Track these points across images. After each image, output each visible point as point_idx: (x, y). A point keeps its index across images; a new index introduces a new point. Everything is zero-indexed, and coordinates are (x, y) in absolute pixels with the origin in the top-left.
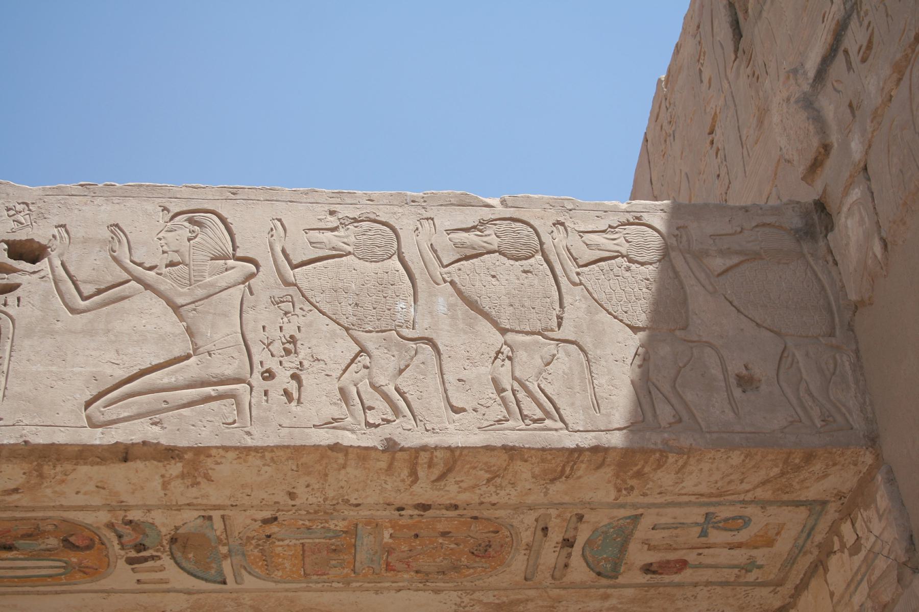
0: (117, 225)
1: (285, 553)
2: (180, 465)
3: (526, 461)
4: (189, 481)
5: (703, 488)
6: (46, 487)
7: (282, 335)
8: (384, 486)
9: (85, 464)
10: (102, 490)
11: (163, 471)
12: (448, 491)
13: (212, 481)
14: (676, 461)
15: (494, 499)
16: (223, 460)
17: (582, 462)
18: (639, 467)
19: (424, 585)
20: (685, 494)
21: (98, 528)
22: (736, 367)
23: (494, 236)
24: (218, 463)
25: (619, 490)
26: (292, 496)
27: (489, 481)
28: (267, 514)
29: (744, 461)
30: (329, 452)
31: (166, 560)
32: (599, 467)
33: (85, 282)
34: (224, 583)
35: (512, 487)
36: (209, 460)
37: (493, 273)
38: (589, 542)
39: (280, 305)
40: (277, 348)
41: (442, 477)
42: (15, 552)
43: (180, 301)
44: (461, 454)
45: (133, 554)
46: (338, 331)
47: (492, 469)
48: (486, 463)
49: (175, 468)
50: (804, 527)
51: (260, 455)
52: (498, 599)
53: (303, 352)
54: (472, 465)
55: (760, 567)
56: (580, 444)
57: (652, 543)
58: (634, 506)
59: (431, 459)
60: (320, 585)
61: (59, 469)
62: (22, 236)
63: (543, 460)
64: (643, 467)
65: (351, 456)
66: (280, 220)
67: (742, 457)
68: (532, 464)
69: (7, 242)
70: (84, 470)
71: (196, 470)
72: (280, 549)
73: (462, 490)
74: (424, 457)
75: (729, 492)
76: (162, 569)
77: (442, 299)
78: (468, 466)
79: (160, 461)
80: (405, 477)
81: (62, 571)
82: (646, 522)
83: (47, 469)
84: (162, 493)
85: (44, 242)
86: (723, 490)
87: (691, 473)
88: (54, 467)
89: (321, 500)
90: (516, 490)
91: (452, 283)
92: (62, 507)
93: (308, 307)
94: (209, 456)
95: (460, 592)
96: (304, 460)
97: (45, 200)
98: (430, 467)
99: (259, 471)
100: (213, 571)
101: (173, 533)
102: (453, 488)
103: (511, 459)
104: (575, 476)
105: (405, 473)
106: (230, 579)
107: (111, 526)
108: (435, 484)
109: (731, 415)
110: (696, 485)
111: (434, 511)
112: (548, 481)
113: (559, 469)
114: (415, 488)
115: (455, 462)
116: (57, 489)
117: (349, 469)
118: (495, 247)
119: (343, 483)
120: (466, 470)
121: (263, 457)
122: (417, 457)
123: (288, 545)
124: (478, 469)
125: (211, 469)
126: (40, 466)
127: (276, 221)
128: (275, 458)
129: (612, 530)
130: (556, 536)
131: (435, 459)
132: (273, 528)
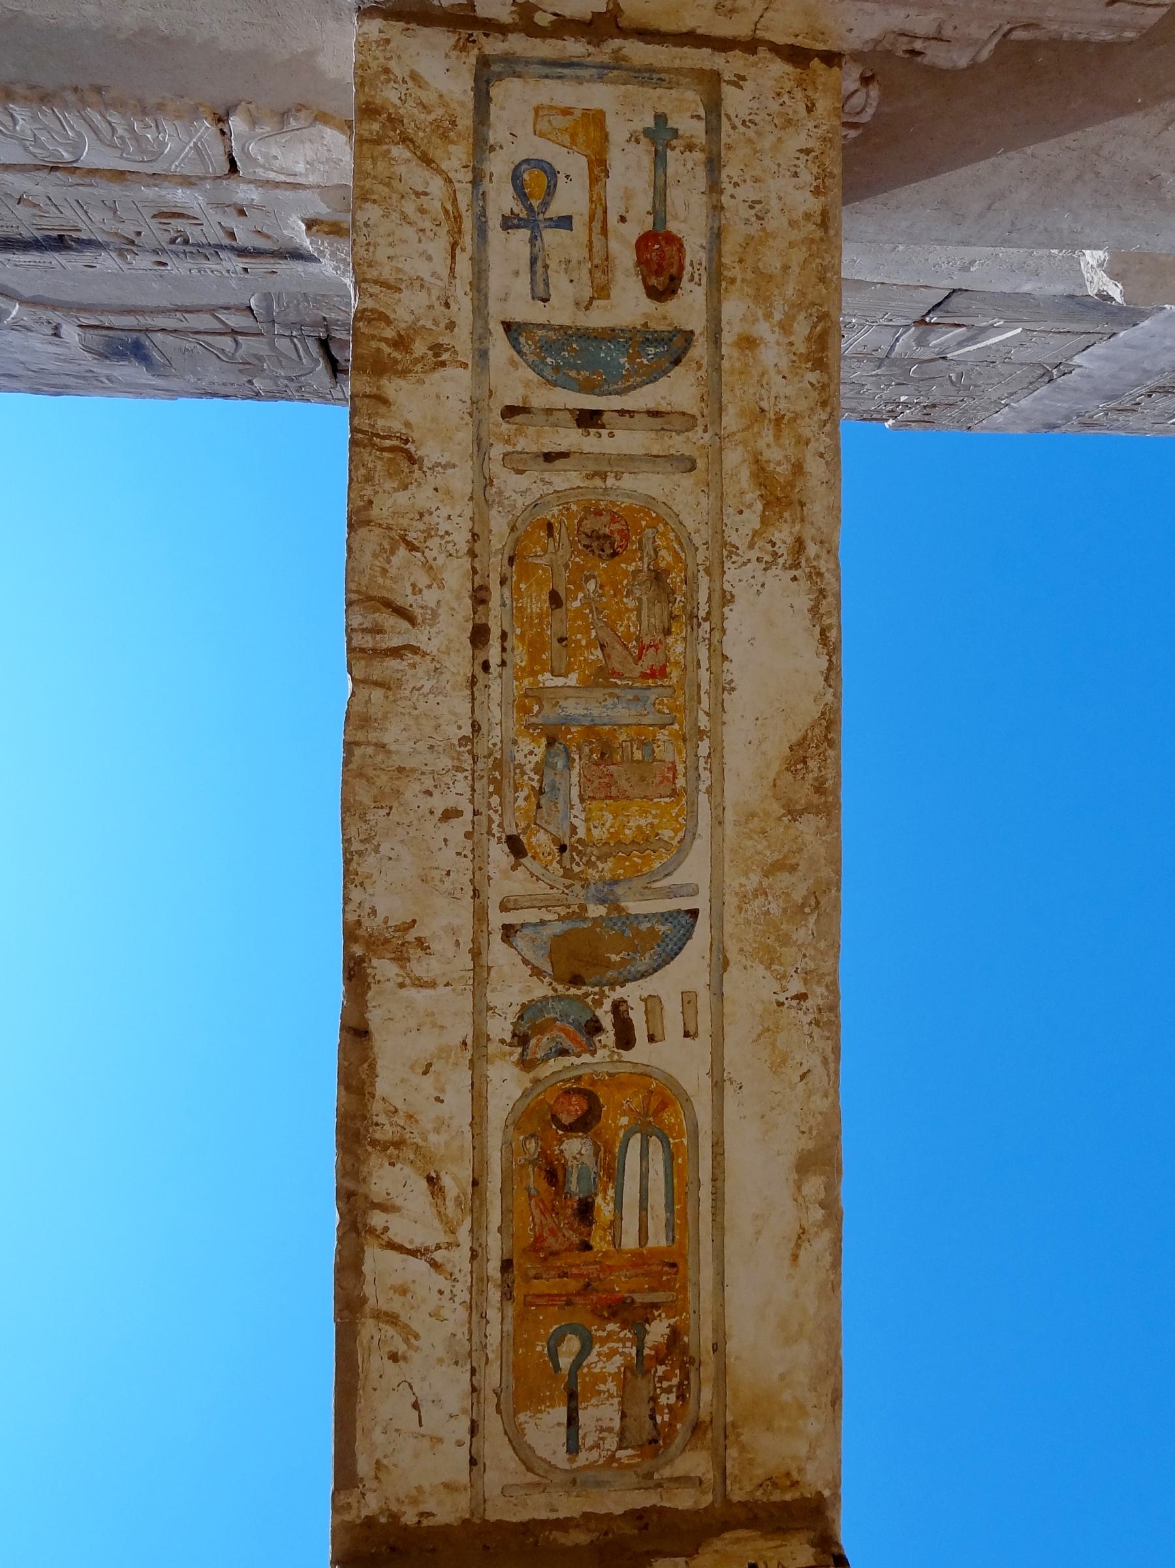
1: (608, 825)
2: (375, 962)
3: (371, 502)
4: (414, 953)
5: (439, 247)
6: (425, 1140)
8: (425, 690)
9: (373, 1085)
10: (432, 1069)
11: (390, 985)
12: (438, 602)
13: (414, 921)
14: (371, 295)
15: (461, 538)
16: (367, 906)
17: (372, 426)
18: (383, 346)
19: (705, 620)
20: (452, 269)
21: (536, 1081)
24: (374, 912)
25: (443, 364)
26: (450, 814)
27: (412, 547)
28: (499, 854)
29: (374, 201)
30: (351, 766)
31: (632, 993)
32: (385, 401)
34: (694, 913)
35: (431, 514)
36: (366, 922)
38: (588, 387)
41: (402, 613)
42: (599, 1200)
44: (358, 592)
45: (608, 1037)
47: (387, 547)
48: (375, 556)
49: (383, 968)
50: (547, 77)
51: (356, 857)
52: (750, 506)
54: (378, 574)
55: (660, 118)
57: (588, 292)
58: (481, 336)
59: (364, 630)
60: (705, 775)
61: (382, 1119)
63: (368, 479)
64: (382, 339)
65: (360, 736)
67: (368, 205)
68: (376, 493)
70: (382, 1087)
71: (387, 941)
72: (596, 833)
73: (437, 581)
74: (361, 640)
75: (449, 207)
76: (652, 1003)
78: (380, 580)
79: (369, 987)
80: (405, 663)
81: (655, 1144)
82: (525, 311)
83: (386, 1133)
84: (441, 989)
86: (442, 216)
87: (398, 270)
88: (377, 1124)
89: (460, 776)
90: (438, 508)
92: (478, 1121)
94: (359, 923)
95: (727, 564)
96: (367, 800)
98: (380, 631)
99: (390, 859)
100: (662, 929)
101: (547, 980)
102: (430, 597)
103: (368, 522)
104: (404, 431)
105: (394, 663)
106: (686, 904)
107: (526, 1064)
108: (419, 620)
110: (429, 258)
111: (491, 617)
112: (416, 466)
113: (386, 455)
114: (431, 647)
115: (370, 598)
116: (430, 1126)
117: (387, 739)
119: (422, 746)
120: (388, 582)
121: (360, 854)
122: (363, 650)
123: (587, 820)
124: (387, 566)
125: (386, 922)
126: (374, 1143)
128: (362, 837)
129: (549, 360)
130: (570, 438)
131: (365, 626)
132: (540, 840)
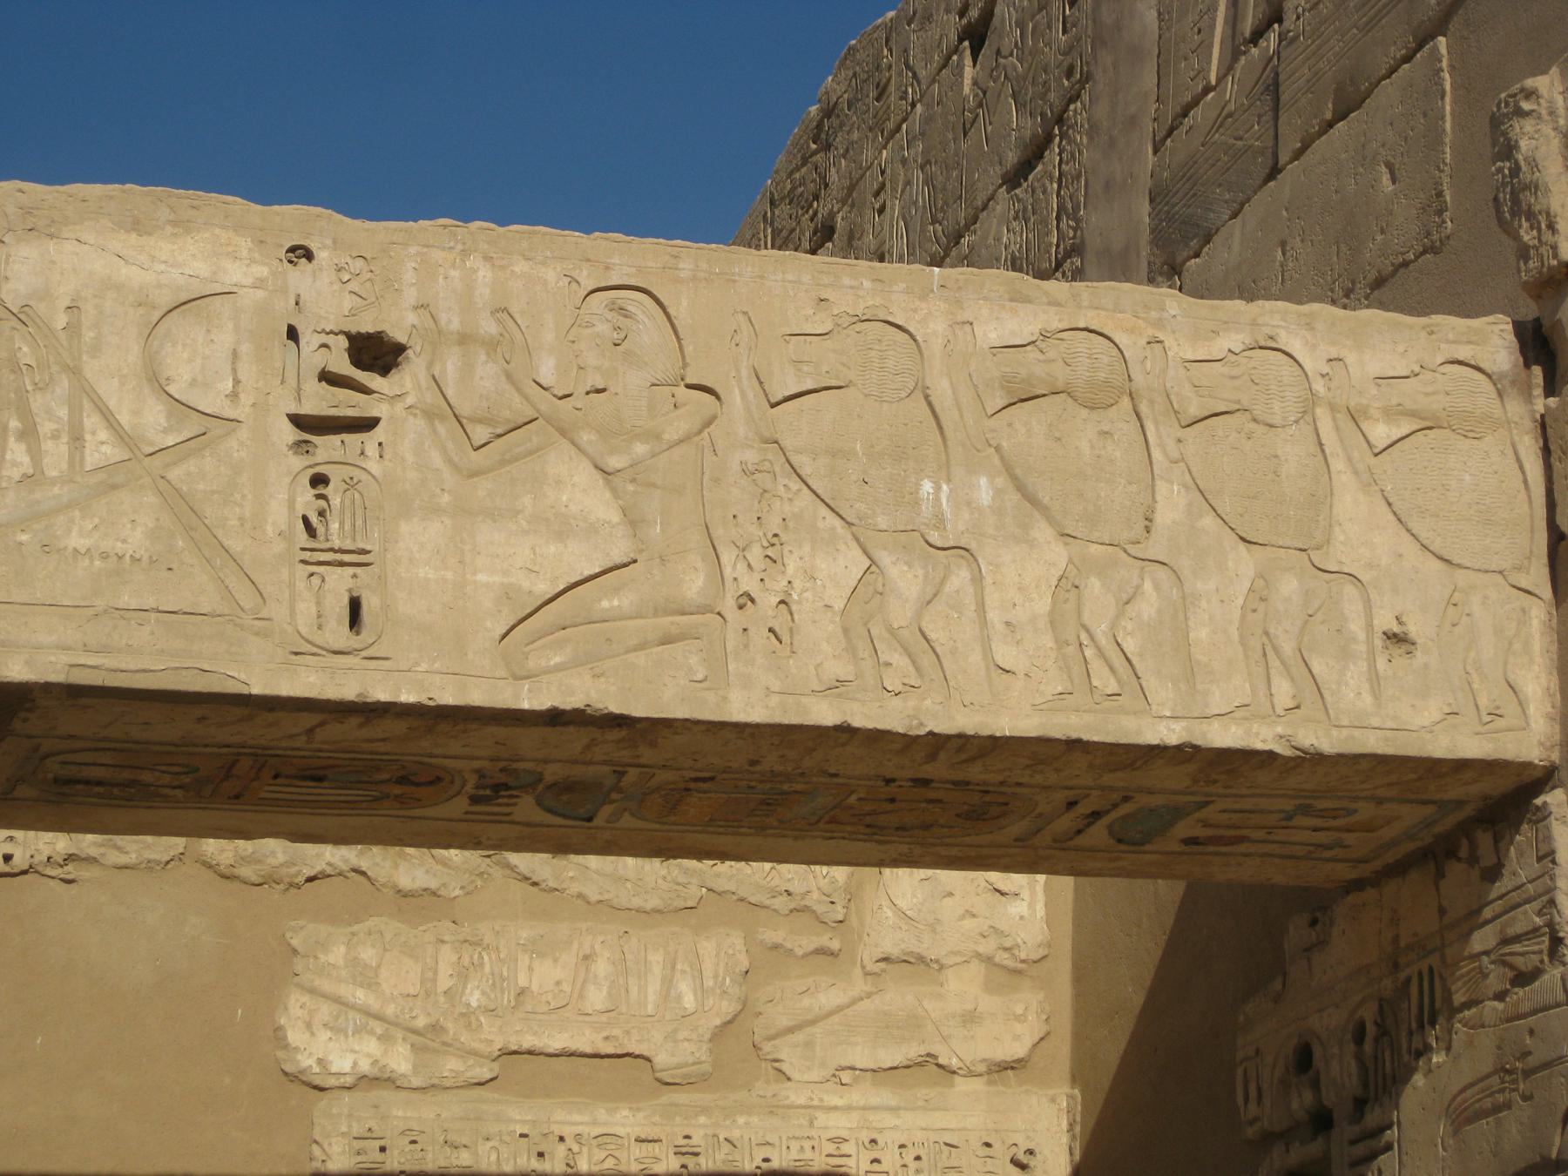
0: (505, 310)
7: (761, 534)
22: (1385, 621)
23: (1061, 363)
33: (472, 420)
37: (1057, 434)
39: (755, 477)
40: (755, 554)
43: (614, 462)
46: (839, 530)
53: (792, 566)
56: (1165, 738)
62: (367, 326)
66: (745, 313)
69: (349, 335)
77: (985, 479)
85: (401, 338)
91: (998, 449)
93: (795, 485)
97: (392, 254)
109: (1368, 699)
118: (1060, 385)
127: (740, 315)
